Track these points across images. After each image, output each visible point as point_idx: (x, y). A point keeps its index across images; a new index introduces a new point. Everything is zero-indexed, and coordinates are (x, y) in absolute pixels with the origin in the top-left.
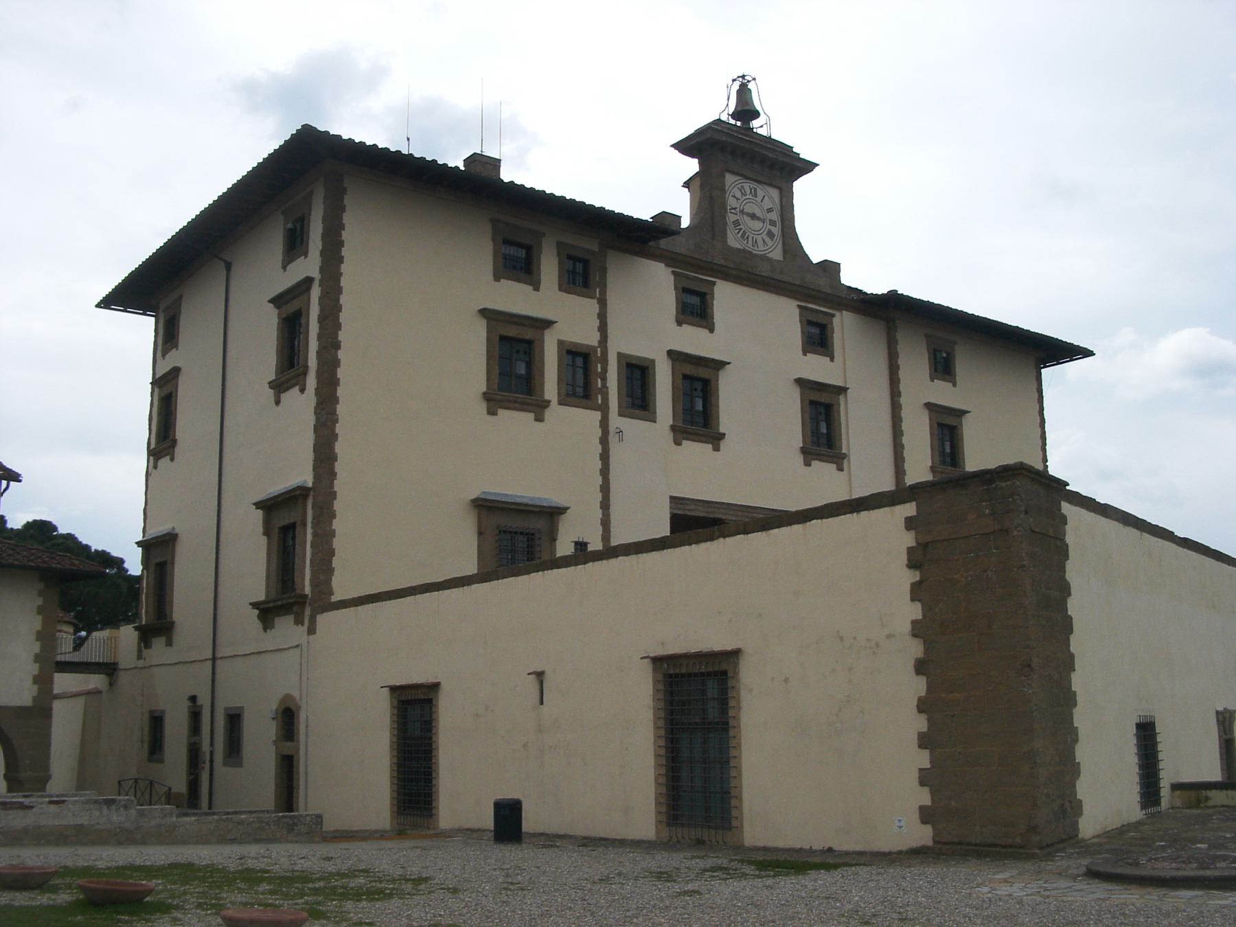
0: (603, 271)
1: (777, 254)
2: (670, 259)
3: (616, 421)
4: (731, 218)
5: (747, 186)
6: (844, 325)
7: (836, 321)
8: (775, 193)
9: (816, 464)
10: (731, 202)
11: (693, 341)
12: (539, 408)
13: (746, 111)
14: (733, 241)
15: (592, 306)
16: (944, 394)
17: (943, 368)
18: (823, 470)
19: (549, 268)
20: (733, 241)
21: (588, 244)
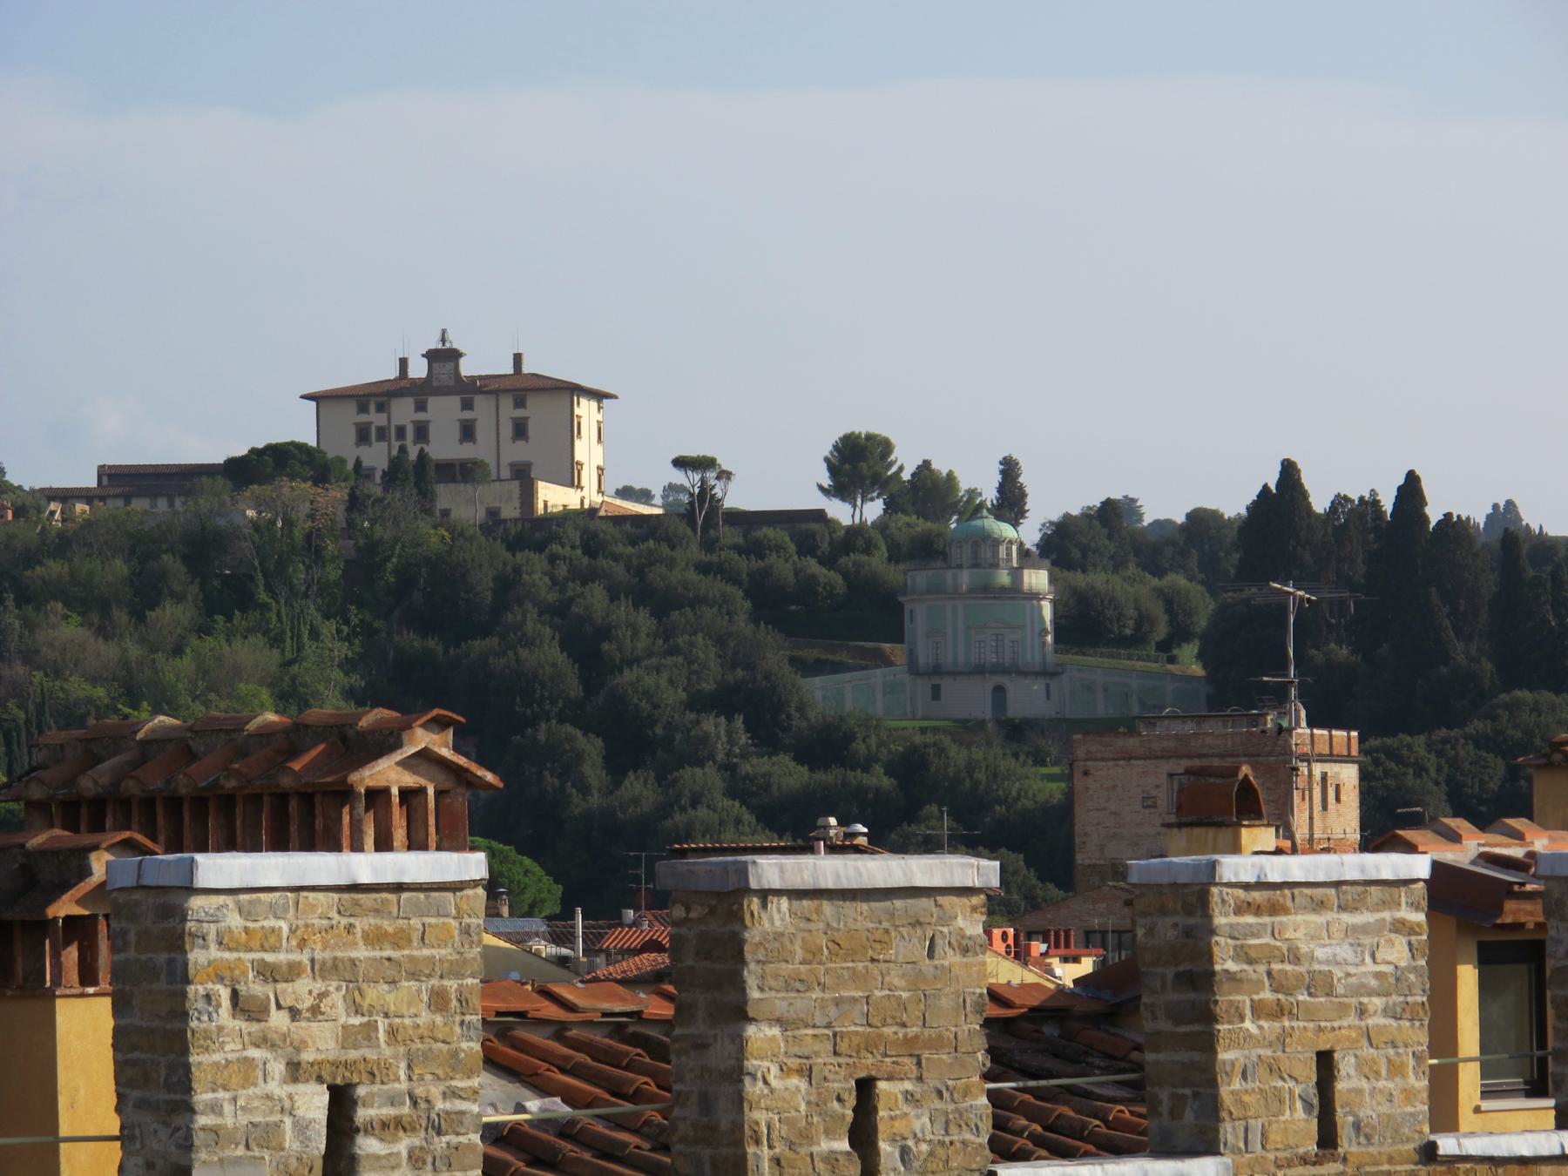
1: (452, 383)
2: (411, 395)
5: (441, 365)
6: (480, 402)
8: (452, 364)
9: (465, 444)
10: (435, 372)
11: (421, 416)
12: (370, 445)
13: (443, 340)
14: (435, 384)
16: (520, 413)
17: (520, 403)
18: (468, 446)
19: (372, 408)
20: (435, 384)
21: (385, 399)
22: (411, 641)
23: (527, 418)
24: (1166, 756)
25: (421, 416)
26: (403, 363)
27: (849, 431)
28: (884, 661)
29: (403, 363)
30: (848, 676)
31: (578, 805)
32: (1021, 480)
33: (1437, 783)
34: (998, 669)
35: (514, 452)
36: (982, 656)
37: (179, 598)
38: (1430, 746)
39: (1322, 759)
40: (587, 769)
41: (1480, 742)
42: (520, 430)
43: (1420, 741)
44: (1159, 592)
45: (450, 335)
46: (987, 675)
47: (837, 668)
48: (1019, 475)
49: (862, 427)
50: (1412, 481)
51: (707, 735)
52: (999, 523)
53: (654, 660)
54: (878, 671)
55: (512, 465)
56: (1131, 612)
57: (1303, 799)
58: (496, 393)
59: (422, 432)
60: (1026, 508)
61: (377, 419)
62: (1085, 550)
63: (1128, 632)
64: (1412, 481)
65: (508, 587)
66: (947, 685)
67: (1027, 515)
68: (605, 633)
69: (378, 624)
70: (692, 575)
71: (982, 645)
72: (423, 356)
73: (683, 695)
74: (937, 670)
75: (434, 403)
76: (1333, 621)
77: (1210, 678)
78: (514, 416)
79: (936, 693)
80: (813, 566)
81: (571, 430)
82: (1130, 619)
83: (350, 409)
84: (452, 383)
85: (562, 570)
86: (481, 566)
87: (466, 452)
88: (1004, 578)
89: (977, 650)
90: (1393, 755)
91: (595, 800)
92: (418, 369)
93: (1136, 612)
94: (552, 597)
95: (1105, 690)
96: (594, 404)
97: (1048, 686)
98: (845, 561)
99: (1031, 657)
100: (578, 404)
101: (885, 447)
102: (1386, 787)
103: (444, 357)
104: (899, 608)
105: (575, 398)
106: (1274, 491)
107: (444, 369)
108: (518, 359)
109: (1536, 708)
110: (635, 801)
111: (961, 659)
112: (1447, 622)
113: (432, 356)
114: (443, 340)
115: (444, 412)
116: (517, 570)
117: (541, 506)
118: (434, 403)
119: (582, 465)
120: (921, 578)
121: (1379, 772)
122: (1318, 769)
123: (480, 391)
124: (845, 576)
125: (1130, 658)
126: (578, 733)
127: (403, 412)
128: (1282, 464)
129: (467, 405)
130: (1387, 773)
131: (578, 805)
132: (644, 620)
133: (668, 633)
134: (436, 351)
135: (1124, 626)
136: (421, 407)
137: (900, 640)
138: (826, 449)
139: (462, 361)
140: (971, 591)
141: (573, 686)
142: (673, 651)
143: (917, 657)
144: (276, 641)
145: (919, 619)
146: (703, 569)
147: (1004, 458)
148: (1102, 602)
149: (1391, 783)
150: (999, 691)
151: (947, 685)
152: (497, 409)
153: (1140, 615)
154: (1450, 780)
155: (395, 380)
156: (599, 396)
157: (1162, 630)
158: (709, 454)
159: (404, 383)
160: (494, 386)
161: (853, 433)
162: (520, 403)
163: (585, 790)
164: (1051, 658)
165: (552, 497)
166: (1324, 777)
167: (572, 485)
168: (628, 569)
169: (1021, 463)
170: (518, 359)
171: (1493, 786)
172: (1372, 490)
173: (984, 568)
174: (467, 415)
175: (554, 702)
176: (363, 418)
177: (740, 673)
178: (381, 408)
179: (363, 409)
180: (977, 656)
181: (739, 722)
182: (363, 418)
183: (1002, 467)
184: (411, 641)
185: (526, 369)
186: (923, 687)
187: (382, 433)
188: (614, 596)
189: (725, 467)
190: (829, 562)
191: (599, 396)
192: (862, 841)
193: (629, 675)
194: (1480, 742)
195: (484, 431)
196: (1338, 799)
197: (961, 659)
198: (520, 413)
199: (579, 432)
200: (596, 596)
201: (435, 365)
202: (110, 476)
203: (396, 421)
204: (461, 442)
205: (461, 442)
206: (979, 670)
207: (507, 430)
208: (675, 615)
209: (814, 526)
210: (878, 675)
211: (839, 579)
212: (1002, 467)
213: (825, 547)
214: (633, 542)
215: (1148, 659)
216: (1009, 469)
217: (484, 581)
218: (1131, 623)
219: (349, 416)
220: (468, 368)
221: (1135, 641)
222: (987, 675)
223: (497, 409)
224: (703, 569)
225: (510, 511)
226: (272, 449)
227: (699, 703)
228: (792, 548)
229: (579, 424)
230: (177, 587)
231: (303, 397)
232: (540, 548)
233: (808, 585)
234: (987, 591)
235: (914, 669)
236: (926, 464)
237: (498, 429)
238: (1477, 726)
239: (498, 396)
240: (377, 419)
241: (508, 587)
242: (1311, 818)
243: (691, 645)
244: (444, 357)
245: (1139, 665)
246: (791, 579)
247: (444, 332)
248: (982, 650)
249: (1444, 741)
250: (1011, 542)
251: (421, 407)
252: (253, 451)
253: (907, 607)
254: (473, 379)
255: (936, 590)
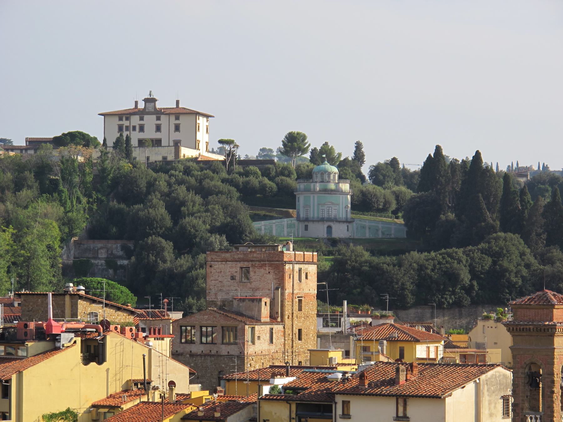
0: (130, 118)
1: (153, 110)
3: (131, 132)
4: (147, 108)
5: (149, 104)
6: (163, 117)
7: (161, 116)
8: (153, 104)
11: (142, 122)
13: (150, 95)
14: (147, 110)
15: (129, 122)
16: (177, 122)
17: (177, 118)
18: (158, 133)
19: (124, 119)
20: (147, 110)
21: (128, 116)
22: (114, 204)
23: (180, 124)
24: (239, 260)
25: (142, 122)
26: (136, 103)
27: (291, 131)
28: (288, 215)
29: (136, 103)
30: (274, 221)
31: (162, 266)
32: (363, 150)
33: (465, 266)
34: (329, 220)
35: (176, 136)
36: (323, 215)
37: (30, 187)
38: (464, 253)
39: (299, 263)
40: (166, 254)
41: (483, 251)
42: (177, 128)
43: (460, 251)
44: (394, 193)
45: (153, 93)
46: (325, 222)
47: (272, 218)
48: (362, 148)
49: (295, 130)
50: (478, 154)
51: (212, 242)
52: (331, 166)
53: (199, 214)
54: (285, 220)
55: (174, 141)
56: (382, 200)
57: (290, 278)
58: (169, 114)
59: (142, 129)
60: (364, 160)
61: (126, 123)
62: (384, 176)
63: (381, 207)
64: (478, 154)
65: (151, 185)
66: (311, 225)
67: (364, 163)
68: (183, 203)
69: (103, 198)
70: (219, 183)
71: (323, 210)
72: (143, 100)
73: (208, 227)
74: (307, 220)
75: (146, 117)
76: (450, 205)
77: (406, 225)
78: (175, 123)
79: (306, 228)
80: (266, 181)
81: (196, 128)
82: (382, 202)
83: (117, 118)
84: (153, 110)
85: (173, 180)
86: (142, 178)
87: (157, 136)
88: (332, 186)
89: (322, 213)
90: (450, 255)
91: (168, 264)
92: (141, 105)
93: (384, 200)
94: (166, 190)
95: (369, 228)
96: (205, 119)
97: (348, 226)
98: (278, 179)
99: (342, 215)
100: (199, 119)
101: (304, 138)
102: (447, 267)
103: (150, 101)
104: (294, 197)
105: (197, 117)
106: (433, 157)
107: (150, 105)
108: (178, 102)
109: (505, 239)
110: (181, 266)
111: (316, 215)
112: (485, 206)
113: (146, 101)
114: (150, 95)
115: (150, 121)
116: (155, 180)
117: (182, 155)
118: (146, 117)
119: (199, 141)
120: (302, 186)
121: (444, 262)
122: (297, 267)
123: (163, 114)
124: (277, 184)
125: (381, 216)
126: (163, 241)
127: (135, 120)
128: (436, 147)
129: (158, 119)
130: (447, 262)
131: (162, 266)
132: (198, 199)
133: (206, 204)
134: (148, 99)
135: (379, 205)
136: (142, 119)
137: (295, 209)
138: (283, 138)
139: (157, 103)
140: (320, 191)
141: (169, 222)
142: (207, 211)
143: (300, 215)
144: (63, 204)
145: (301, 200)
146: (224, 181)
147: (357, 142)
148: (371, 196)
149: (448, 265)
150: (329, 228)
151: (311, 225)
152: (169, 120)
153: (385, 201)
154: (470, 265)
155: (133, 109)
156: (207, 116)
157: (394, 206)
158: (232, 139)
159: (136, 110)
160: (168, 112)
161: (292, 132)
162: (177, 118)
163: (165, 261)
164: (349, 215)
165: (187, 152)
166: (300, 270)
167: (196, 148)
168: (196, 180)
169: (363, 144)
170: (178, 102)
171: (487, 268)
172: (467, 157)
173: (325, 183)
174: (158, 122)
175: (161, 229)
176: (121, 123)
177: (229, 219)
178: (127, 119)
179: (121, 119)
180: (322, 215)
181: (224, 237)
182: (121, 123)
183: (356, 145)
184: (114, 204)
185: (180, 106)
186: (302, 226)
187: (127, 128)
188: (188, 190)
189: (237, 144)
190: (271, 179)
191: (207, 116)
192: (82, 293)
193: (187, 219)
194: (483, 251)
195: (164, 128)
196: (307, 278)
197: (316, 215)
198: (177, 122)
199: (199, 130)
200: (181, 191)
201: (147, 104)
202: (29, 142)
203: (132, 124)
204: (156, 132)
205: (156, 132)
206: (322, 220)
207: (173, 128)
208: (210, 197)
209: (270, 166)
210: (285, 221)
211: (274, 185)
212: (356, 145)
213: (273, 173)
214: (202, 169)
215: (388, 217)
216: (358, 146)
217: (143, 184)
218: (382, 204)
219: (116, 122)
220: (159, 105)
221: (383, 210)
222: (325, 222)
223: (169, 120)
224: (224, 181)
225: (171, 157)
226: (70, 134)
227: (213, 230)
228: (259, 173)
229: (199, 126)
230: (30, 183)
231: (99, 114)
232: (166, 172)
233: (263, 187)
234: (326, 191)
235: (298, 219)
236: (326, 144)
237: (169, 127)
238: (482, 245)
239: (169, 116)
240: (125, 123)
241: (151, 185)
242: (293, 285)
243: (214, 209)
244: (150, 101)
245: (384, 219)
246: (258, 185)
247: (150, 92)
248: (323, 213)
249: (470, 251)
250: (335, 173)
251: (142, 119)
252: (64, 134)
253: (297, 196)
254: (161, 109)
255: (308, 190)
